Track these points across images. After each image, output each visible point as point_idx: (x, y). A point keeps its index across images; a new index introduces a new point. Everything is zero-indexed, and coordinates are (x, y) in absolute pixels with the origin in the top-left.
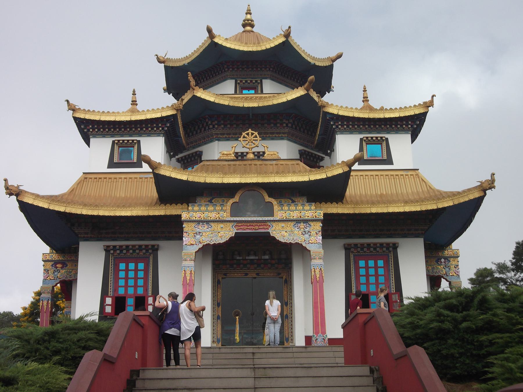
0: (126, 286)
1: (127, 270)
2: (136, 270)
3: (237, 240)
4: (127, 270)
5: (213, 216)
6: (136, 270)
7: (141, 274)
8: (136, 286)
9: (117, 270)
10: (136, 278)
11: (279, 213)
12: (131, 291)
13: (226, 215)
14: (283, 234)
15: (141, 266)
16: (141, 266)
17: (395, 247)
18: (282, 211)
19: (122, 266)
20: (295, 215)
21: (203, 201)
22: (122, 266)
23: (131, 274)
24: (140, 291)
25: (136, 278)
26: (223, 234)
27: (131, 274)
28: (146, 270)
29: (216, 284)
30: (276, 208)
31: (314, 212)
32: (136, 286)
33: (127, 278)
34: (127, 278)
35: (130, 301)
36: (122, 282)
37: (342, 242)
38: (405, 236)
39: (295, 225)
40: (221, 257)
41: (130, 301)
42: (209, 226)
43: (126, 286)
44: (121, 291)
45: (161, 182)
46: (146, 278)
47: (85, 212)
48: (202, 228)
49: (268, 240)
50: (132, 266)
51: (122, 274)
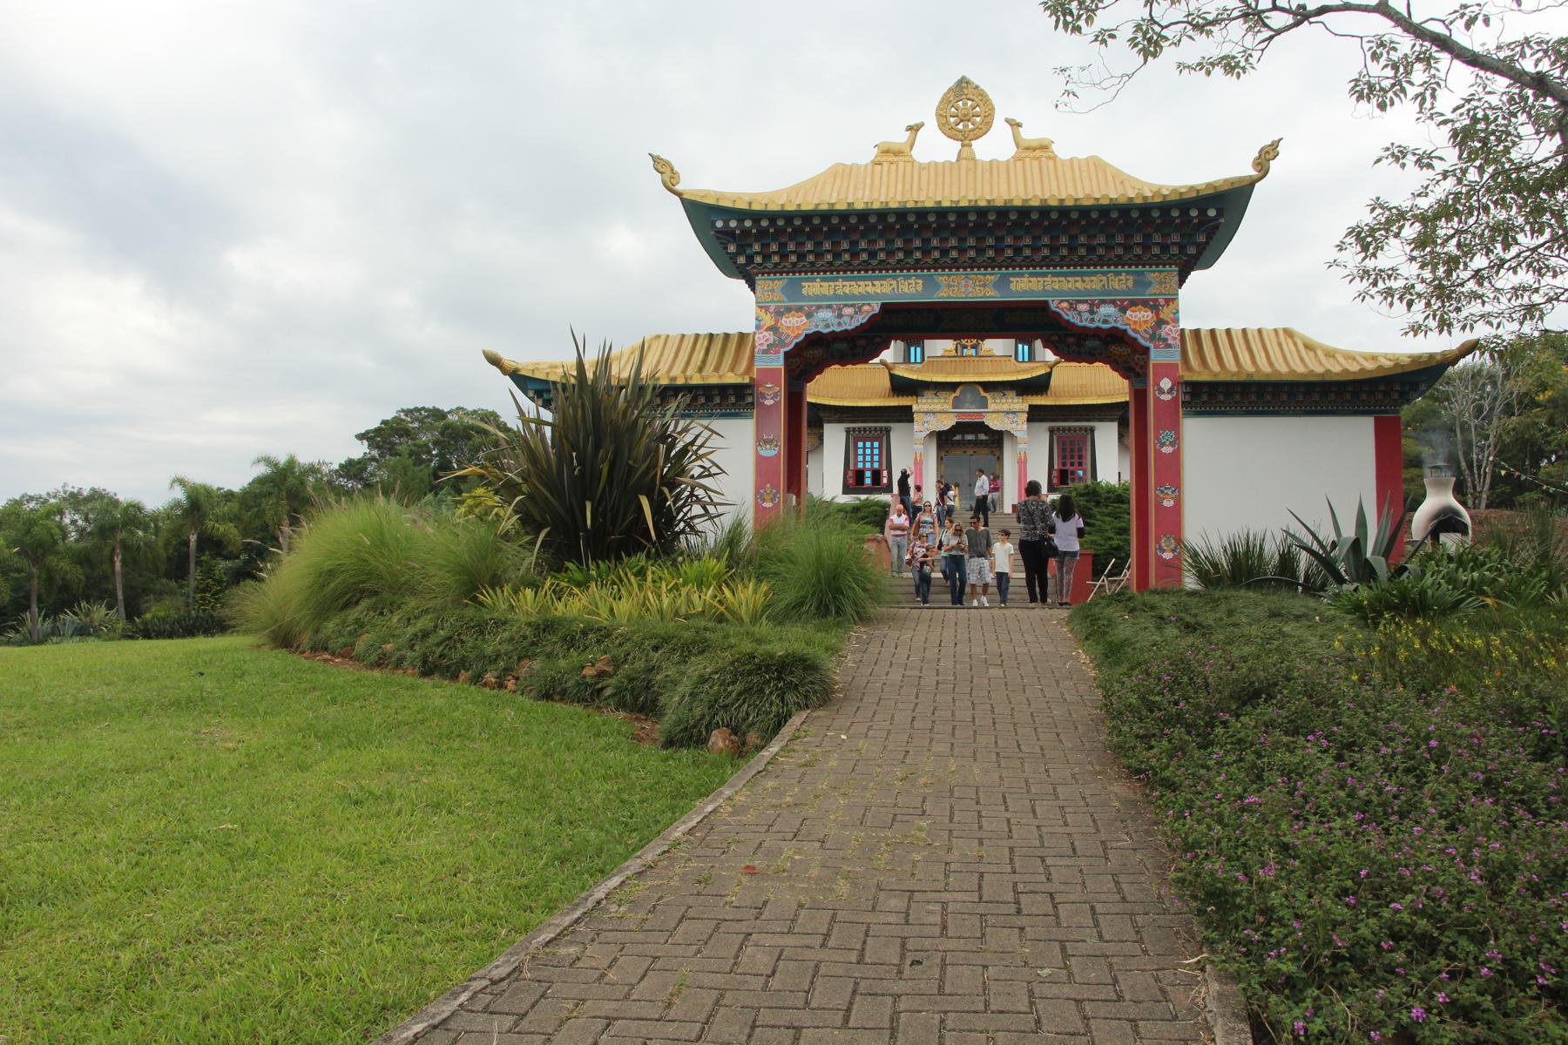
0: (864, 461)
1: (864, 448)
2: (872, 448)
3: (959, 428)
4: (864, 448)
5: (938, 408)
6: (872, 448)
7: (876, 451)
8: (872, 461)
9: (856, 448)
10: (872, 455)
11: (992, 406)
12: (868, 465)
13: (948, 407)
14: (994, 423)
15: (876, 444)
16: (876, 444)
17: (1092, 430)
18: (996, 403)
19: (860, 444)
20: (1005, 407)
21: (929, 394)
22: (860, 444)
23: (868, 451)
24: (876, 465)
25: (872, 455)
26: (946, 423)
27: (868, 451)
28: (880, 448)
29: (940, 459)
30: (990, 401)
31: (1021, 404)
32: (872, 461)
33: (864, 455)
34: (864, 455)
35: (868, 474)
36: (860, 458)
37: (1046, 425)
38: (1101, 420)
39: (1005, 414)
40: (944, 440)
41: (868, 474)
42: (935, 414)
43: (864, 461)
44: (860, 465)
45: (893, 378)
46: (880, 455)
47: (832, 403)
48: (930, 418)
49: (981, 427)
50: (868, 444)
51: (860, 451)
